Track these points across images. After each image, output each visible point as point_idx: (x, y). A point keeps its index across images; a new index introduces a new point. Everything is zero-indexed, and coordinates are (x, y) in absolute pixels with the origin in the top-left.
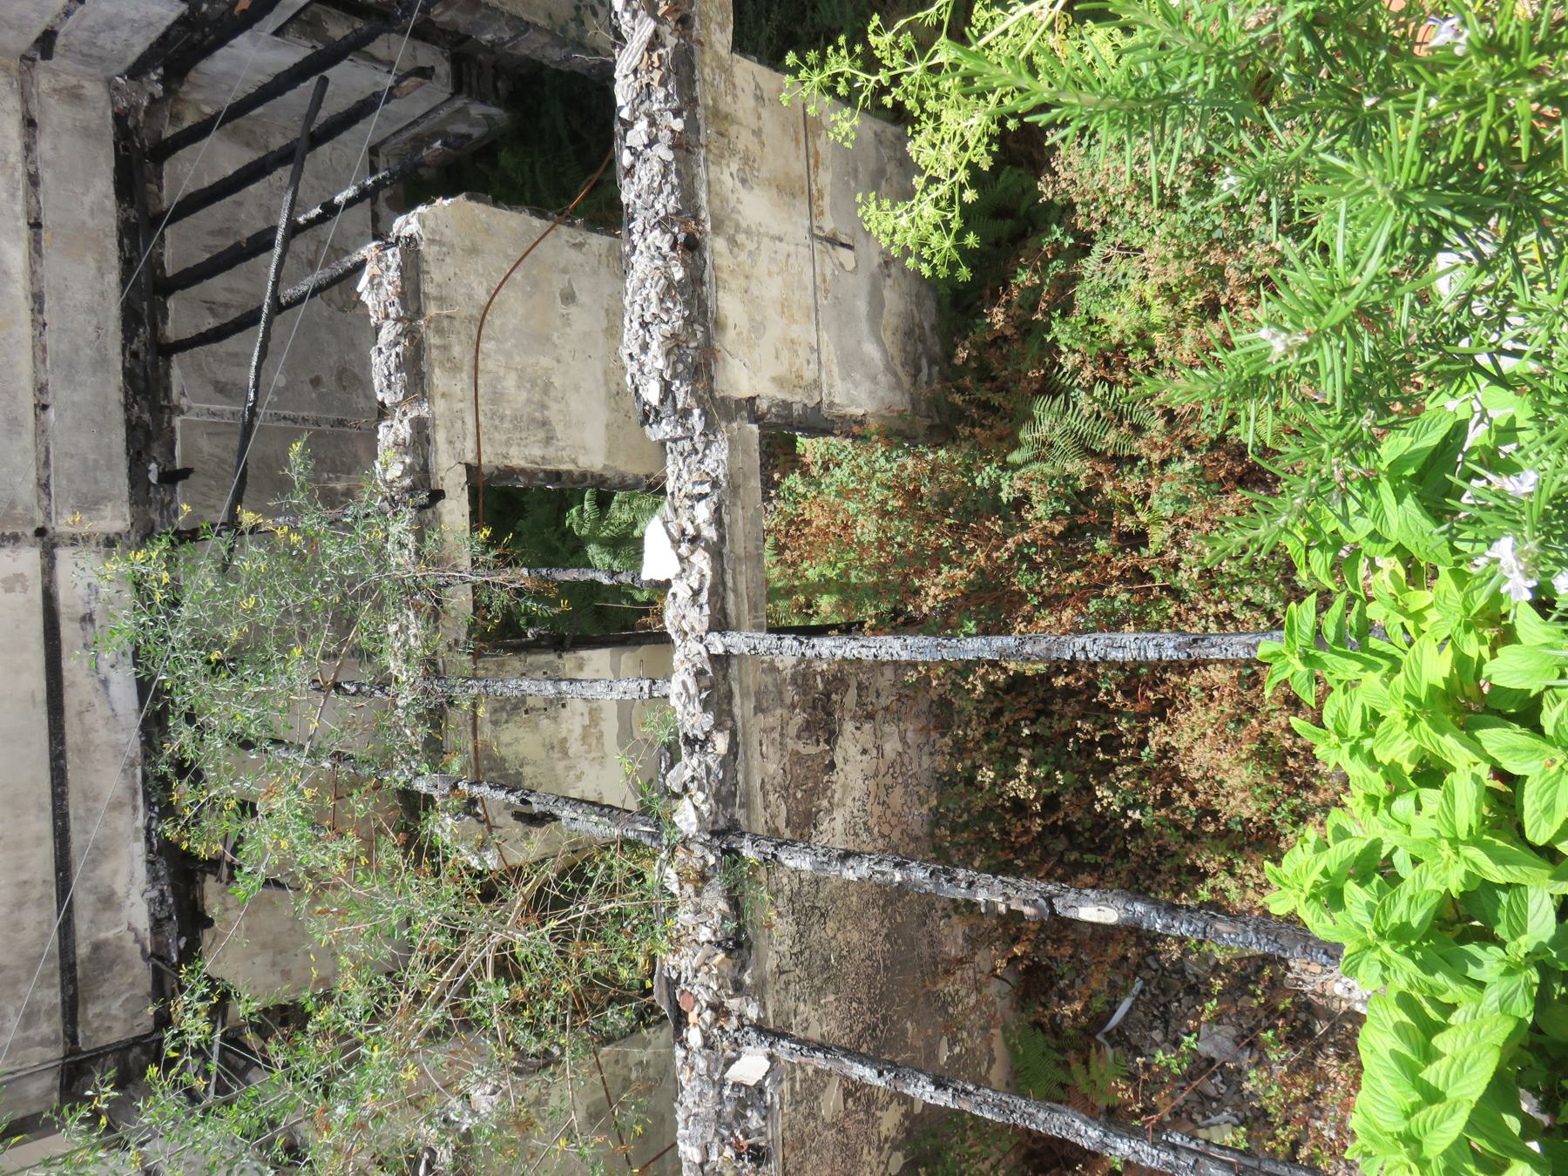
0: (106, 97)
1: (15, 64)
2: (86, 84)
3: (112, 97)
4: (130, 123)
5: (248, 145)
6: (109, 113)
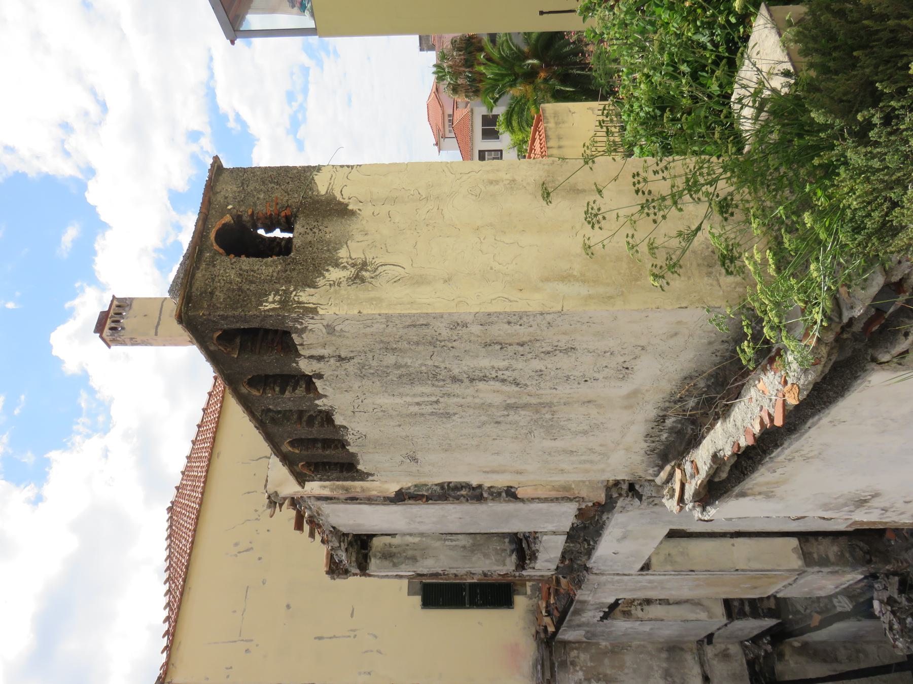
0: (741, 651)
1: (694, 646)
2: (730, 646)
3: (744, 651)
4: (757, 668)
5: (825, 661)
6: (744, 661)
